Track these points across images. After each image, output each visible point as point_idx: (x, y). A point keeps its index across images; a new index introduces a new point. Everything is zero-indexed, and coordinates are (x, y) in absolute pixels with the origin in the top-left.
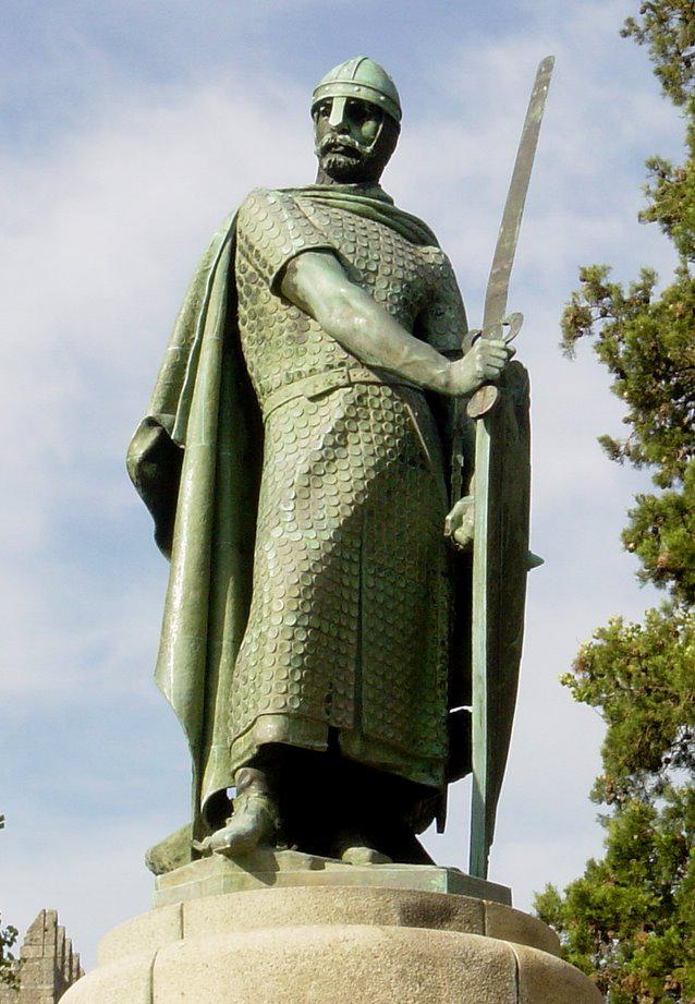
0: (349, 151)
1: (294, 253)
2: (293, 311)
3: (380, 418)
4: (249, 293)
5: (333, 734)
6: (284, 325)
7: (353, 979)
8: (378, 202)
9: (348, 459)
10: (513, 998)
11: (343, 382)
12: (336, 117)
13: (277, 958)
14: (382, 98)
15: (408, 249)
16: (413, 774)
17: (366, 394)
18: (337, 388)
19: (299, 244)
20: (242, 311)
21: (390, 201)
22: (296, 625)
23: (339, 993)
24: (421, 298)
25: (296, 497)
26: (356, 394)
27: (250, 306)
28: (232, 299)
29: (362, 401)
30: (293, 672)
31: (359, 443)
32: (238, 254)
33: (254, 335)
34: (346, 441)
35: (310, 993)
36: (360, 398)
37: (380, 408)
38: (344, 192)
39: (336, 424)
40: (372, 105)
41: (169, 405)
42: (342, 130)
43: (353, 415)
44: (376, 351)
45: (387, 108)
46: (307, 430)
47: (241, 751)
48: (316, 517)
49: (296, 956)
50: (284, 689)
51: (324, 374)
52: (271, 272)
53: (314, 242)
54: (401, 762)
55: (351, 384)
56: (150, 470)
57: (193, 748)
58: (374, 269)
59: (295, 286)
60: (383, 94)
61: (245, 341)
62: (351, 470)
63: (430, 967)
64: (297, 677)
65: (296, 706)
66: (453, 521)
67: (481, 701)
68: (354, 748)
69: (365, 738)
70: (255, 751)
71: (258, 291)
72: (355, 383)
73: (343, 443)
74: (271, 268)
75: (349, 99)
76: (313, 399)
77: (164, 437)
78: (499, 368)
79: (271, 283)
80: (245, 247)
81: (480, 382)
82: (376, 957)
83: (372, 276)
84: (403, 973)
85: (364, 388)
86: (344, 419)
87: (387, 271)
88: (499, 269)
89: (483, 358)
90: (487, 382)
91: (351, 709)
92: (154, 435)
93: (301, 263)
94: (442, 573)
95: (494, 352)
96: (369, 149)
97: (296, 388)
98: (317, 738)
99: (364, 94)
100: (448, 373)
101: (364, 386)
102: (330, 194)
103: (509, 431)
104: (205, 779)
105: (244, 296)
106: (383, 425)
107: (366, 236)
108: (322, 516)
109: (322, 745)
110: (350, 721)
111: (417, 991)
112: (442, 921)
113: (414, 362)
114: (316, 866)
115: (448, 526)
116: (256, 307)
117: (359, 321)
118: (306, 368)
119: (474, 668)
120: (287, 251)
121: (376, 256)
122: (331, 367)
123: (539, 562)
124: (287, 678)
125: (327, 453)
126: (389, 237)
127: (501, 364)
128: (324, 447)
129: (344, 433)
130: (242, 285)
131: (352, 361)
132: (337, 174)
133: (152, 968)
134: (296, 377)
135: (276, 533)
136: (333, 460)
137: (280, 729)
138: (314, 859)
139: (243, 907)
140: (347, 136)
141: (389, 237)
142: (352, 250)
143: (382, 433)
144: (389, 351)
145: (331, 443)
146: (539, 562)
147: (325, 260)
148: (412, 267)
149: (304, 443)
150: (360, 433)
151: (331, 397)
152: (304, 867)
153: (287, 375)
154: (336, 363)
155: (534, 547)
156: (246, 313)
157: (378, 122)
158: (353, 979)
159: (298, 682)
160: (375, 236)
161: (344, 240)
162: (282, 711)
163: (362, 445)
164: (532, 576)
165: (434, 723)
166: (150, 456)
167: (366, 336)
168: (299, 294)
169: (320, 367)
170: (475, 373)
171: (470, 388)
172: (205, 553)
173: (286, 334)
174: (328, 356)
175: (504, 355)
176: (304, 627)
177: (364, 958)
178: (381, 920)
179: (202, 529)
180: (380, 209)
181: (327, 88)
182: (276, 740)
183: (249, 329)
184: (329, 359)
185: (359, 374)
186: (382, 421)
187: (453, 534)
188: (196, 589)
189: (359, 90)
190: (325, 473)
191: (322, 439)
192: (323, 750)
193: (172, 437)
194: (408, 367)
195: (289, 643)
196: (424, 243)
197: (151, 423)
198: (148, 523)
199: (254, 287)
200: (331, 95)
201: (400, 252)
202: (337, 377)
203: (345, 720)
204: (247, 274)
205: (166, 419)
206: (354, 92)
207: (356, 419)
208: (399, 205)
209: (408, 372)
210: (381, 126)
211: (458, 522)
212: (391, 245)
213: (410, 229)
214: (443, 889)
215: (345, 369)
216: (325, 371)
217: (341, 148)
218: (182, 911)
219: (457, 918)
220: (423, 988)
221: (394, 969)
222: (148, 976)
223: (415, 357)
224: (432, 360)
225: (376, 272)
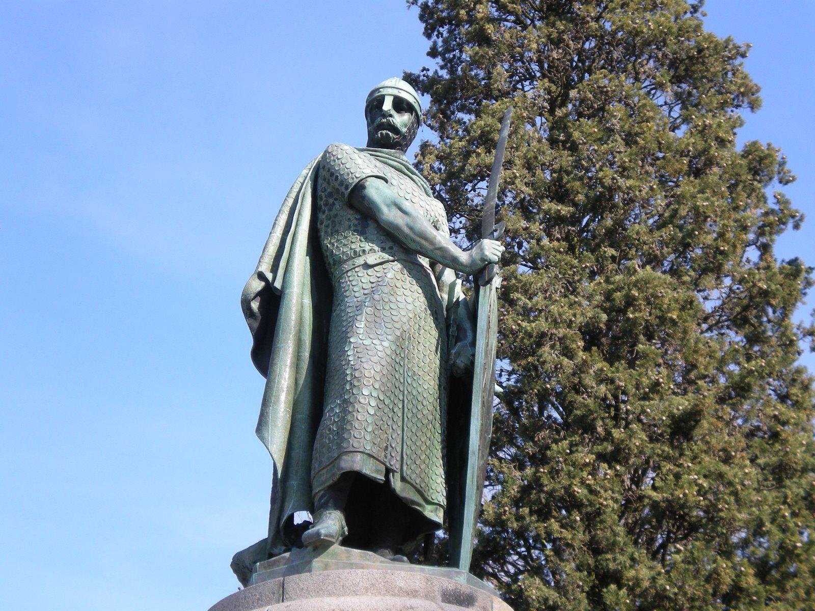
19: (368, 172)
20: (321, 216)
32: (320, 181)
47: (323, 478)
52: (347, 188)
54: (422, 502)
66: (455, 354)
68: (397, 484)
69: (403, 479)
71: (334, 204)
80: (328, 176)
97: (360, 261)
98: (377, 471)
109: (381, 477)
135: (352, 340)
156: (324, 217)
187: (455, 362)
198: (248, 342)
199: (331, 201)
203: (395, 464)
205: (270, 276)
206: (395, 92)
218: (283, 585)
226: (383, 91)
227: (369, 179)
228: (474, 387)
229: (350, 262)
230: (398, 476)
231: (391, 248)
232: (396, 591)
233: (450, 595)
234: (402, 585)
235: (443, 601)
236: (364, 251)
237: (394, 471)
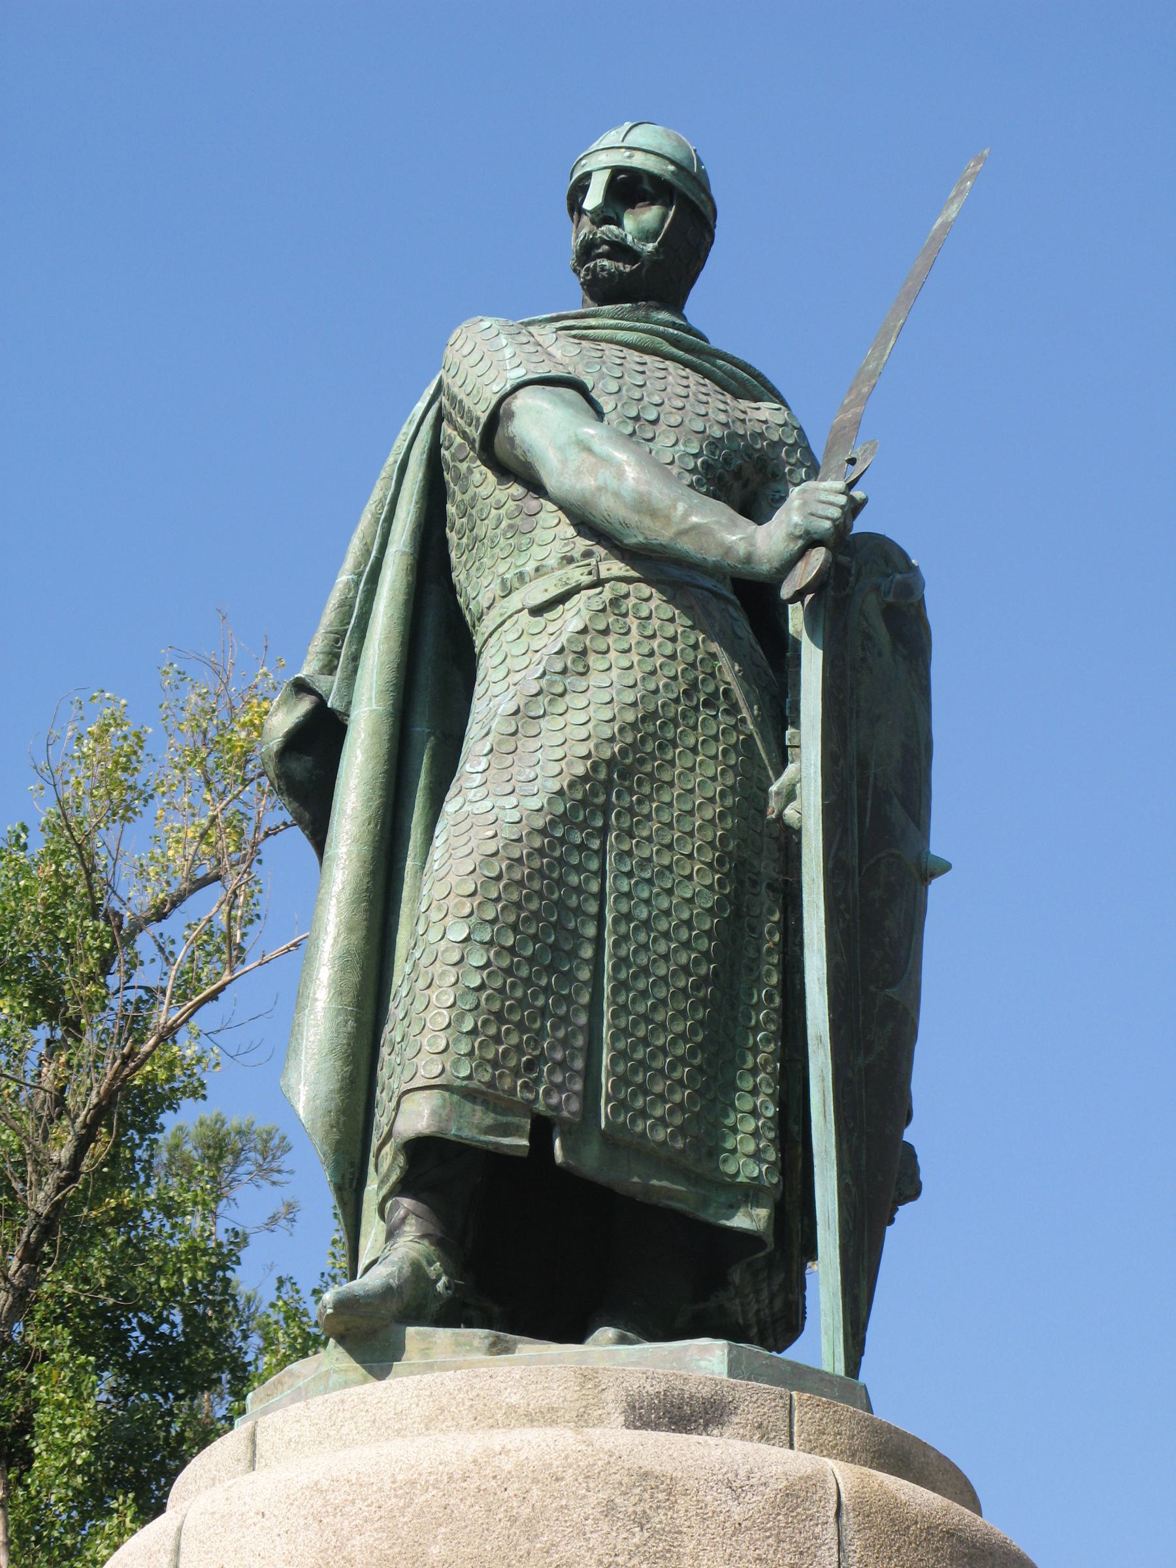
0: (619, 250)
1: (508, 387)
2: (517, 490)
3: (649, 632)
4: (458, 478)
5: (542, 1129)
6: (502, 511)
7: (513, 1520)
8: (671, 330)
9: (589, 694)
10: (829, 1556)
11: (586, 579)
12: (593, 199)
13: (380, 1489)
14: (671, 168)
15: (720, 397)
16: (711, 1211)
17: (627, 596)
18: (576, 590)
19: (517, 375)
21: (706, 341)
22: (467, 939)
23: (488, 1548)
24: (740, 468)
25: (491, 750)
26: (607, 593)
27: (459, 497)
29: (619, 607)
30: (461, 1017)
31: (609, 669)
32: (445, 424)
33: (465, 540)
34: (587, 669)
35: (434, 1550)
36: (615, 602)
37: (649, 618)
38: (613, 318)
39: (568, 640)
40: (654, 178)
41: (329, 668)
42: (602, 217)
43: (602, 627)
44: (633, 518)
46: (525, 661)
48: (522, 779)
49: (413, 1483)
50: (442, 1045)
51: (558, 573)
53: (542, 371)
55: (599, 583)
56: (300, 766)
57: (339, 1189)
58: (652, 417)
59: (511, 440)
60: (673, 162)
61: (453, 555)
62: (592, 708)
63: (662, 1496)
64: (468, 1025)
65: (464, 1073)
66: (778, 793)
67: (823, 1080)
70: (401, 1160)
72: (608, 580)
73: (581, 670)
74: (478, 419)
75: (616, 171)
77: (321, 702)
78: (833, 520)
79: (477, 445)
81: (800, 543)
82: (557, 1480)
83: (649, 427)
84: (609, 1509)
85: (623, 588)
86: (584, 631)
87: (675, 419)
88: (852, 397)
89: (805, 504)
90: (811, 542)
91: (578, 1086)
92: (305, 705)
93: (524, 401)
94: (770, 887)
95: (823, 497)
96: (650, 247)
97: (515, 601)
98: (506, 1130)
99: (639, 161)
100: (750, 540)
101: (624, 585)
102: (592, 322)
103: (868, 637)
104: (362, 1241)
105: (452, 485)
106: (655, 644)
107: (643, 373)
108: (532, 776)
110: (575, 1106)
111: (636, 1540)
112: (706, 1425)
113: (695, 527)
114: (497, 1348)
115: (773, 804)
116: (467, 497)
117: (605, 476)
118: (530, 568)
119: (809, 1023)
120: (499, 387)
121: (657, 399)
122: (570, 560)
123: (946, 867)
124: (449, 1025)
125: (552, 683)
126: (687, 378)
127: (836, 513)
128: (544, 674)
129: (583, 653)
130: (448, 469)
131: (600, 551)
133: (180, 1530)
134: (516, 585)
136: (562, 695)
137: (433, 1113)
138: (498, 1337)
139: (348, 1415)
140: (613, 227)
141: (687, 378)
142: (616, 389)
143: (651, 654)
144: (653, 513)
145: (559, 667)
146: (946, 867)
147: (559, 396)
148: (722, 418)
149: (516, 677)
150: (612, 655)
151: (568, 605)
152: (478, 1349)
153: (503, 582)
154: (577, 554)
155: (939, 845)
157: (668, 206)
158: (513, 1520)
159: (469, 1033)
160: (661, 374)
161: (602, 376)
162: (437, 1081)
163: (615, 672)
164: (937, 889)
165: (750, 1125)
166: (296, 741)
167: (617, 495)
168: (519, 452)
169: (552, 562)
170: (791, 529)
171: (786, 555)
172: (373, 874)
173: (504, 525)
174: (566, 545)
175: (842, 500)
176: (481, 943)
177: (536, 1481)
178: (582, 1419)
179: (367, 838)
180: (675, 342)
181: (583, 162)
182: (427, 1132)
183: (458, 532)
184: (568, 548)
185: (615, 568)
186: (653, 636)
187: (780, 816)
188: (350, 930)
189: (630, 157)
190: (543, 716)
191: (544, 663)
192: (525, 1153)
193: (329, 705)
194: (685, 538)
195: (453, 970)
200: (588, 169)
201: (704, 398)
202: (577, 575)
204: (452, 449)
205: (322, 684)
207: (605, 632)
208: (715, 343)
209: (687, 546)
210: (671, 213)
211: (790, 795)
212: (687, 387)
213: (732, 376)
214: (720, 1374)
215: (593, 561)
216: (561, 566)
217: (605, 248)
218: (254, 1434)
219: (735, 1419)
220: (646, 1535)
221: (593, 1499)
222: (170, 1545)
223: (694, 519)
224: (724, 521)
225: (654, 422)
226: (588, 165)
227: (521, 393)
228: (804, 870)
229: (494, 612)
231: (587, 554)
232: (499, 1416)
233: (651, 1407)
234: (514, 1399)
235: (630, 1425)
236: (521, 576)
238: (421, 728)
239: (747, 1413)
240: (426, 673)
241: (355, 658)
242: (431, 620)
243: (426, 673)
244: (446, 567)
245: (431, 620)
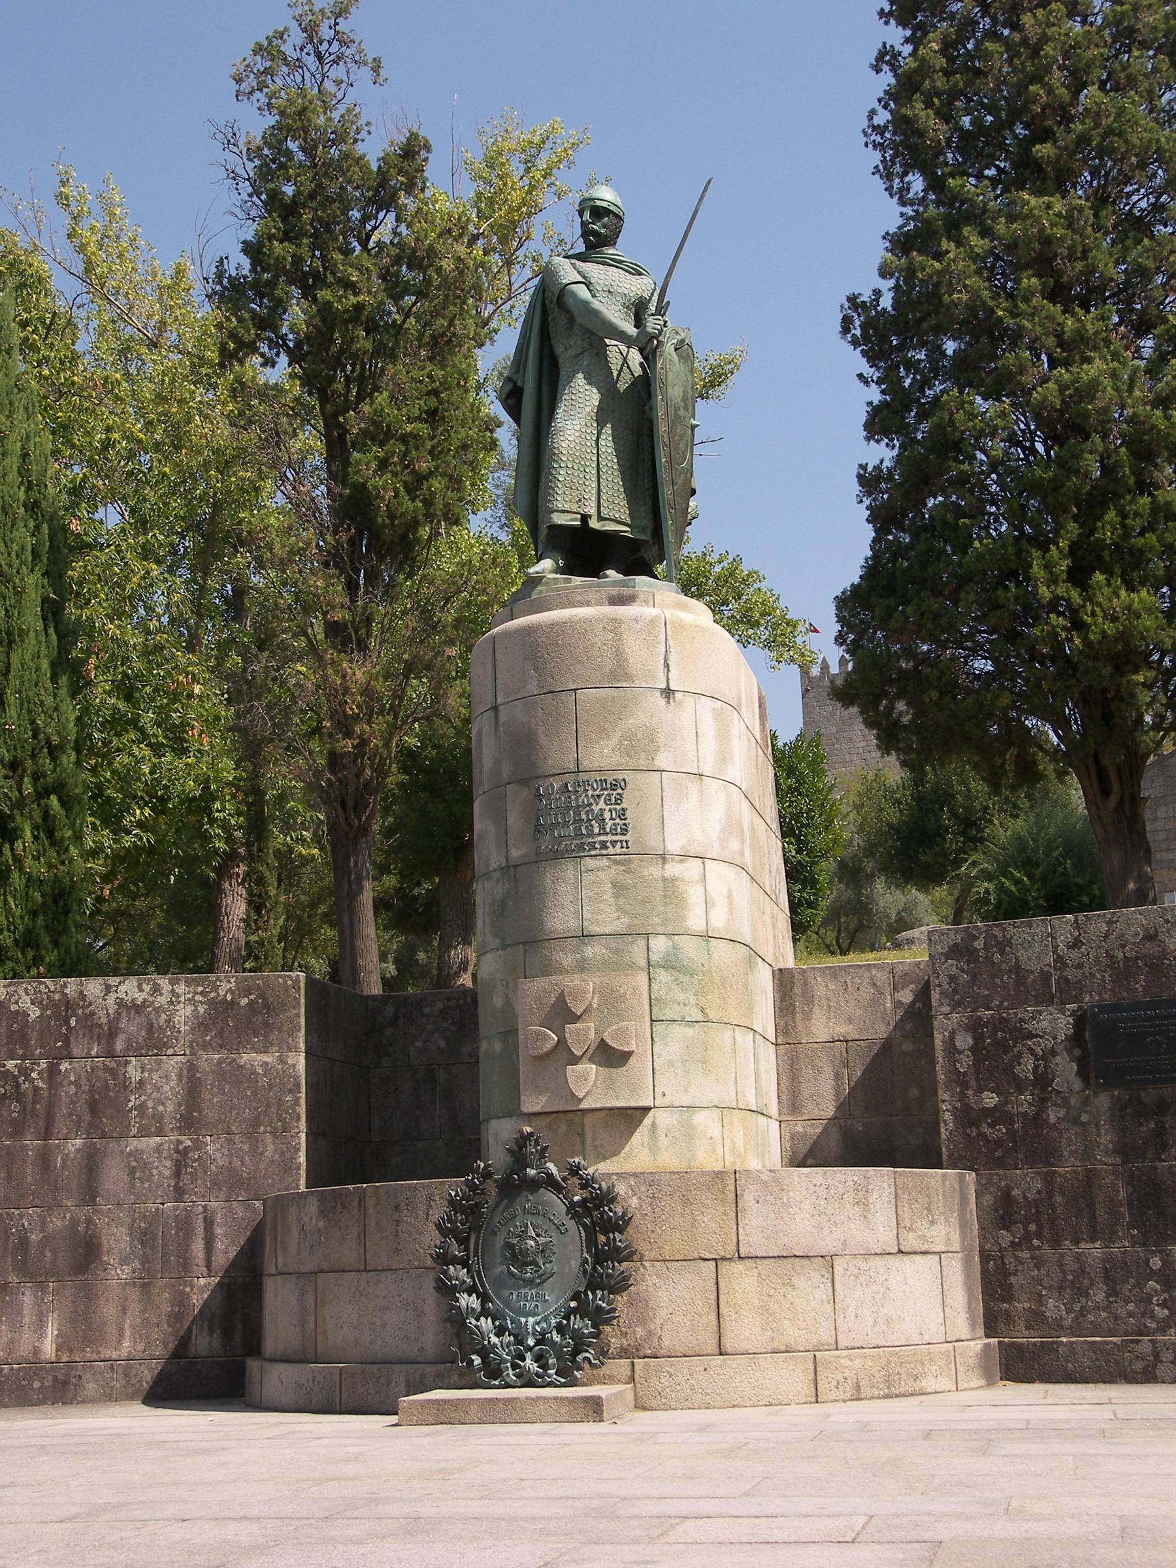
0: (595, 233)
5: (585, 518)
28: (545, 313)
41: (517, 371)
45: (612, 208)
56: (511, 402)
68: (594, 524)
76: (576, 356)
92: (511, 385)
98: (576, 520)
99: (598, 203)
132: (590, 247)
166: (510, 395)
196: (640, 274)
197: (509, 379)
203: (591, 510)
205: (515, 377)
230: (595, 518)
237: (590, 516)
238: (545, 389)
239: (641, 596)
240: (545, 370)
241: (525, 368)
242: (546, 351)
243: (545, 370)
244: (549, 338)
245: (546, 351)
